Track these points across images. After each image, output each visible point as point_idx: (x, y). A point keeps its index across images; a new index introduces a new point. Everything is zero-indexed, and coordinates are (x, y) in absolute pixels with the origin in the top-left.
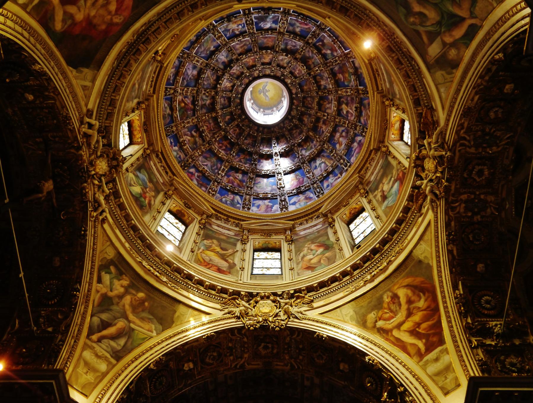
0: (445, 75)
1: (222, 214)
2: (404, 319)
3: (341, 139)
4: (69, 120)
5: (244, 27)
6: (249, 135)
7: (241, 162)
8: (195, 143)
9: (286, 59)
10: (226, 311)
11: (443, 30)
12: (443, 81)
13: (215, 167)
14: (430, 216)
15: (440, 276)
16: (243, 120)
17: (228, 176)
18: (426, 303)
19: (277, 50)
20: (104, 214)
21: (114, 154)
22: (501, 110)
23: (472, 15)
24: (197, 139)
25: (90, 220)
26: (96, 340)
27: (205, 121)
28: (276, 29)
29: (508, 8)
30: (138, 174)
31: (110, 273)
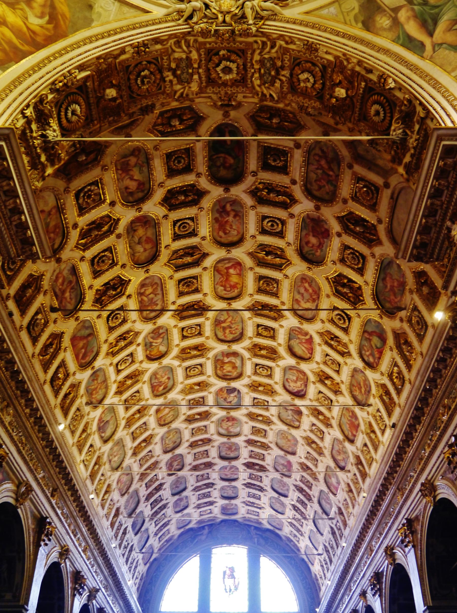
11: (416, 7)
12: (344, 10)
15: (85, 42)
18: (38, 28)
22: (309, 85)
23: (436, 46)
29: (451, 90)
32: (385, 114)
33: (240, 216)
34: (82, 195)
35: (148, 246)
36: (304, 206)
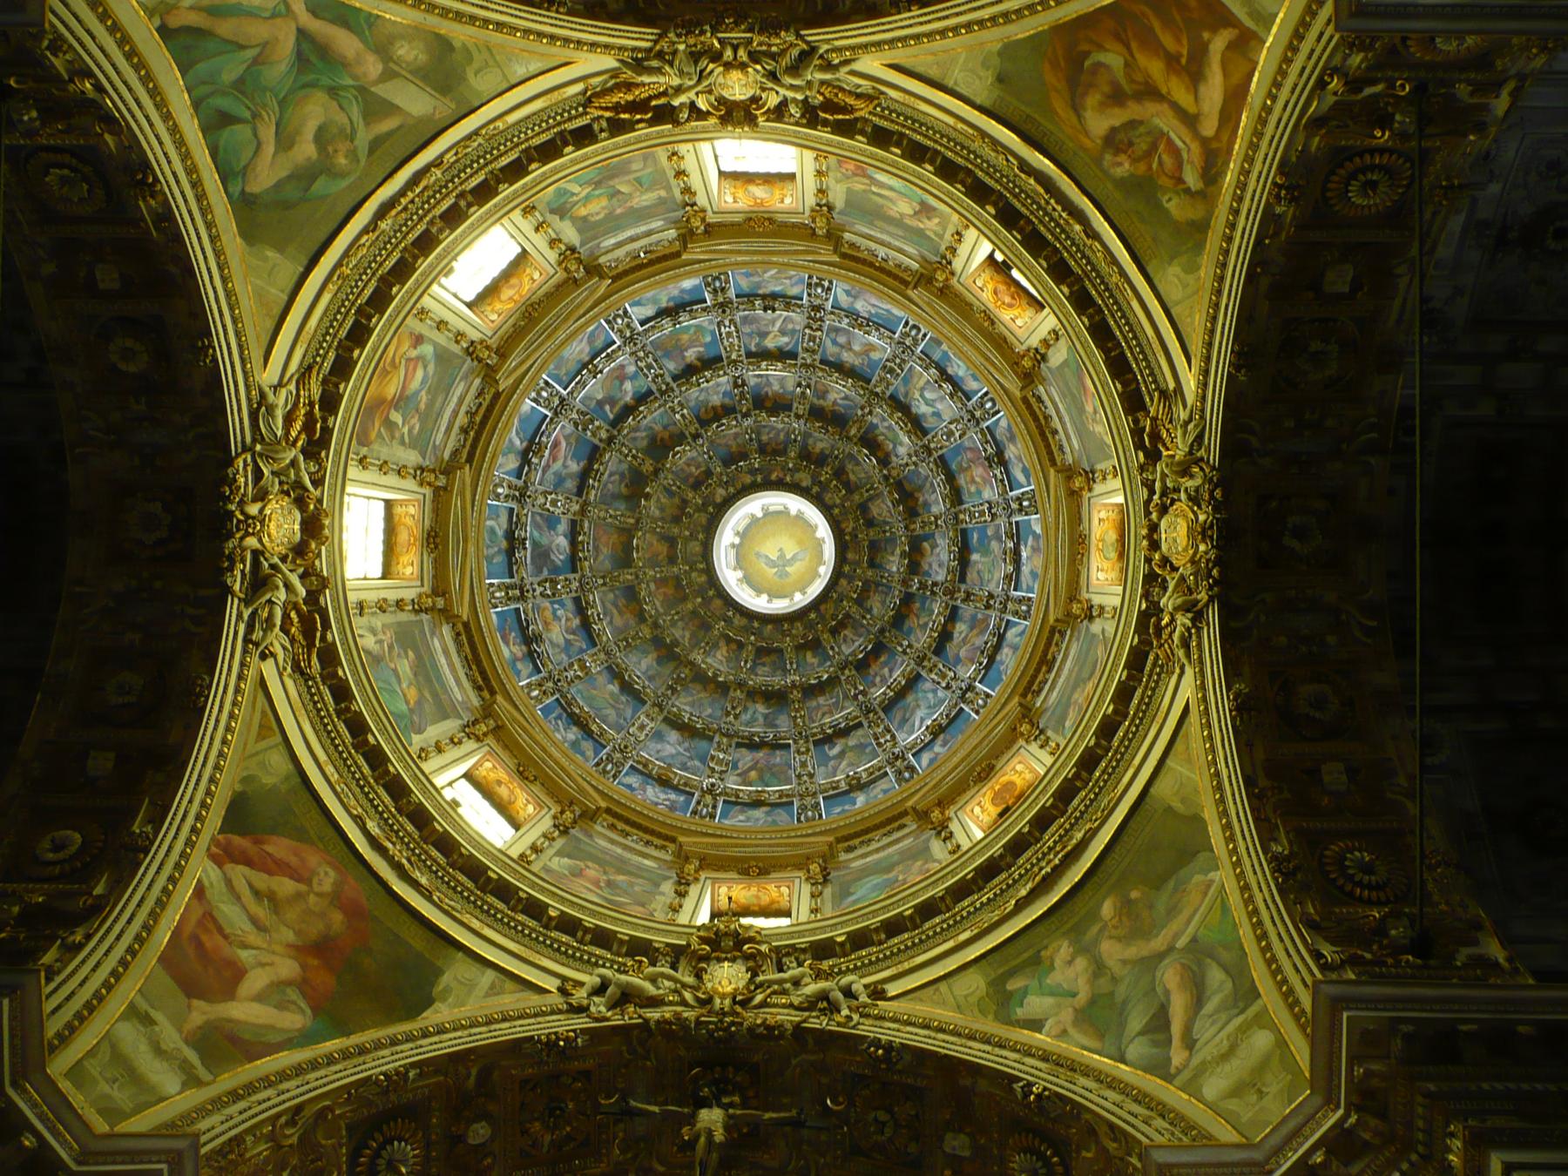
0: (475, 65)
1: (1034, 677)
3: (857, 348)
4: (558, 1039)
5: (562, 605)
6: (860, 602)
7: (926, 624)
8: (861, 747)
9: (658, 500)
10: (1181, 653)
11: (351, 82)
14: (871, 64)
16: (822, 617)
17: (958, 660)
19: (632, 521)
20: (857, 987)
21: (703, 940)
25: (854, 1027)
26: (1187, 1053)
28: (573, 523)
31: (1025, 992)
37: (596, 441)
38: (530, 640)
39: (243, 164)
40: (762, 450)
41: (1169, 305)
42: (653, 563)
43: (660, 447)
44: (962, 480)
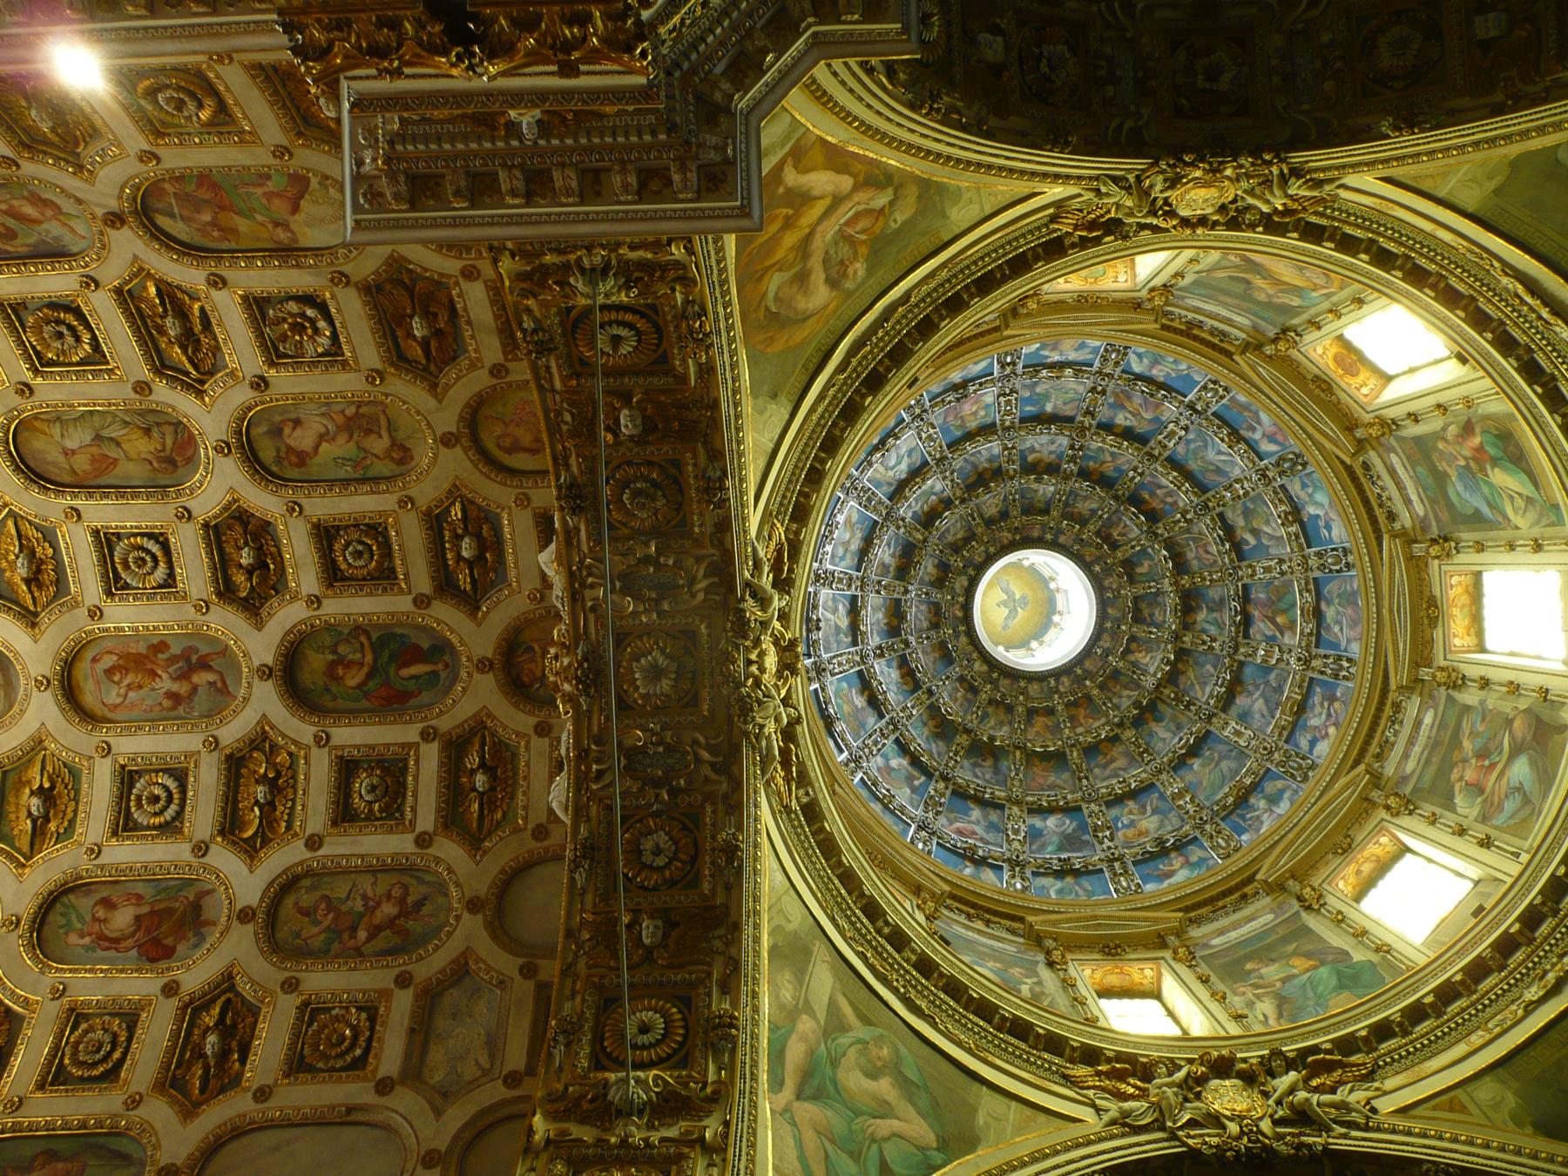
0: (784, 923)
2: (819, 229)
5: (1117, 819)
6: (1083, 521)
7: (1112, 454)
8: (1247, 514)
10: (1327, 188)
13: (1192, 446)
17: (1156, 420)
24: (1241, 522)
27: (1211, 565)
28: (1031, 811)
30: (1486, 510)
32: (651, 1045)
33: (174, 708)
34: (310, 312)
35: (82, 463)
36: (243, 880)
37: (948, 793)
38: (1163, 850)
39: (913, 1150)
40: (935, 626)
41: (982, 216)
42: (1056, 730)
43: (943, 728)
44: (972, 425)
